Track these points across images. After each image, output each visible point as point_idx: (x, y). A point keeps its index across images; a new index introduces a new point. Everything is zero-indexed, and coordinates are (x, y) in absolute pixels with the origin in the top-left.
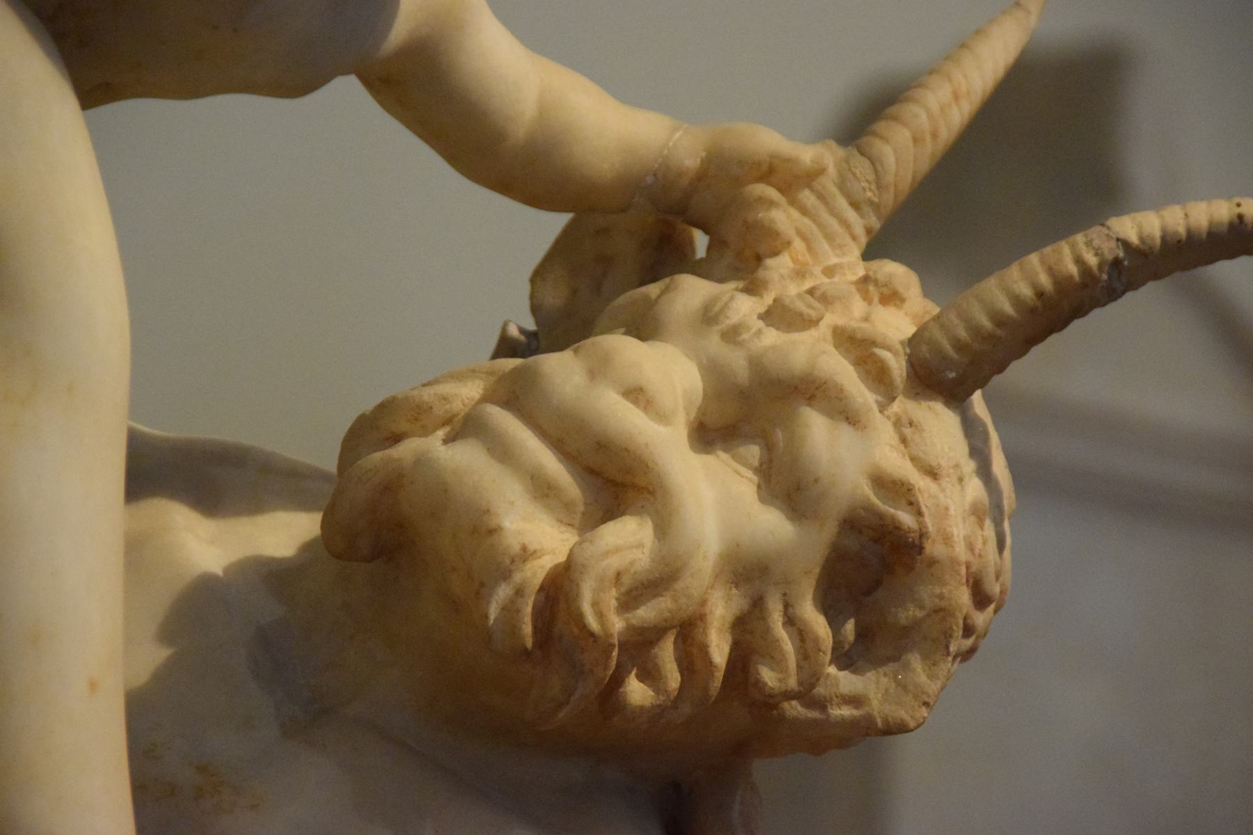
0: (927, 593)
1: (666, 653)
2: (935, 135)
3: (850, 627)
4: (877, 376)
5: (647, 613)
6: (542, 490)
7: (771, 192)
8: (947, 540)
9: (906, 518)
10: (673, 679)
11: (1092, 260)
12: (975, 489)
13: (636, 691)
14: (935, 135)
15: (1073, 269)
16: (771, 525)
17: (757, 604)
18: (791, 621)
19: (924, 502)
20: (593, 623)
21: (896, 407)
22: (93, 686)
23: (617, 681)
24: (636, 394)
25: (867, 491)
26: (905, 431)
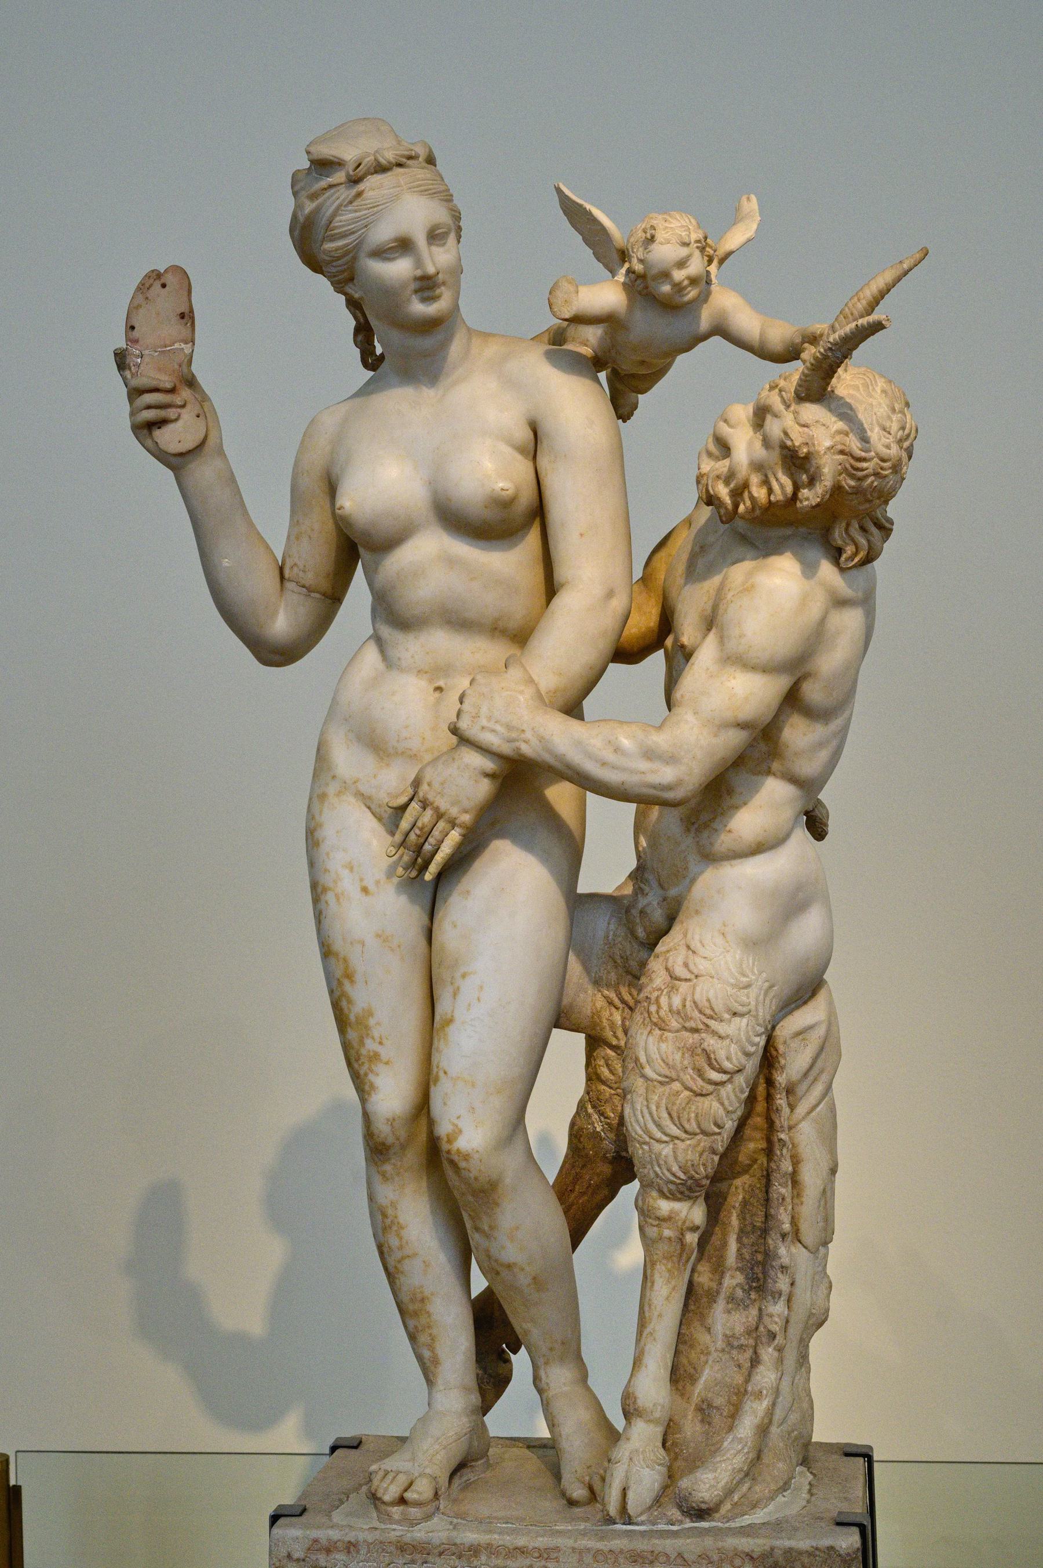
0: (814, 462)
1: (746, 494)
2: (852, 314)
3: (804, 477)
4: (784, 402)
5: (732, 486)
6: (710, 454)
7: (806, 345)
8: (814, 445)
9: (789, 443)
10: (748, 503)
11: (822, 350)
12: (840, 425)
13: (742, 508)
14: (852, 314)
15: (818, 355)
16: (760, 452)
17: (766, 476)
18: (777, 480)
19: (793, 436)
20: (712, 492)
21: (792, 408)
22: (581, 535)
23: (736, 506)
24: (726, 421)
25: (782, 435)
26: (796, 413)
